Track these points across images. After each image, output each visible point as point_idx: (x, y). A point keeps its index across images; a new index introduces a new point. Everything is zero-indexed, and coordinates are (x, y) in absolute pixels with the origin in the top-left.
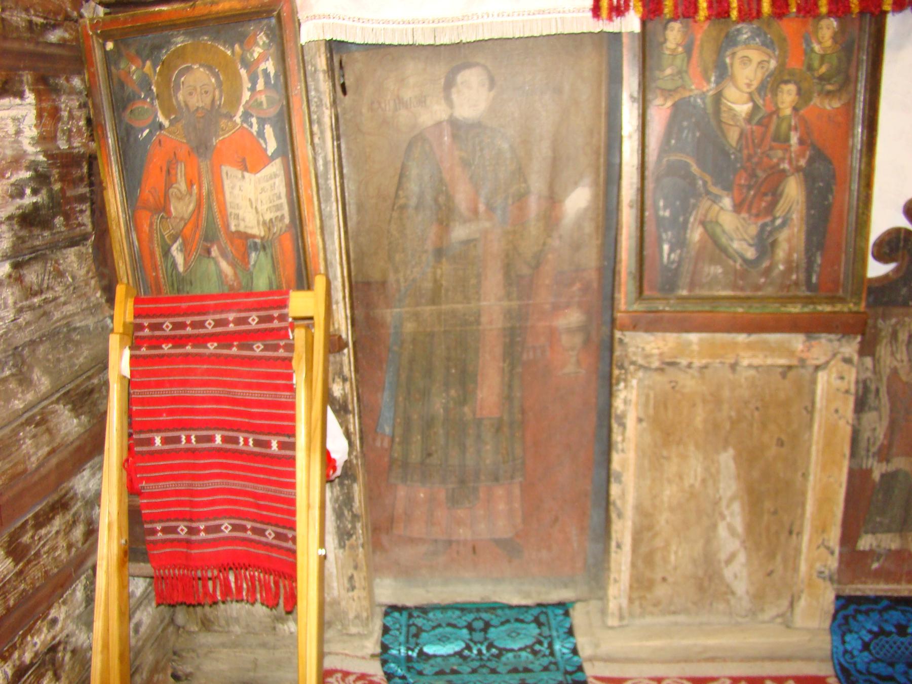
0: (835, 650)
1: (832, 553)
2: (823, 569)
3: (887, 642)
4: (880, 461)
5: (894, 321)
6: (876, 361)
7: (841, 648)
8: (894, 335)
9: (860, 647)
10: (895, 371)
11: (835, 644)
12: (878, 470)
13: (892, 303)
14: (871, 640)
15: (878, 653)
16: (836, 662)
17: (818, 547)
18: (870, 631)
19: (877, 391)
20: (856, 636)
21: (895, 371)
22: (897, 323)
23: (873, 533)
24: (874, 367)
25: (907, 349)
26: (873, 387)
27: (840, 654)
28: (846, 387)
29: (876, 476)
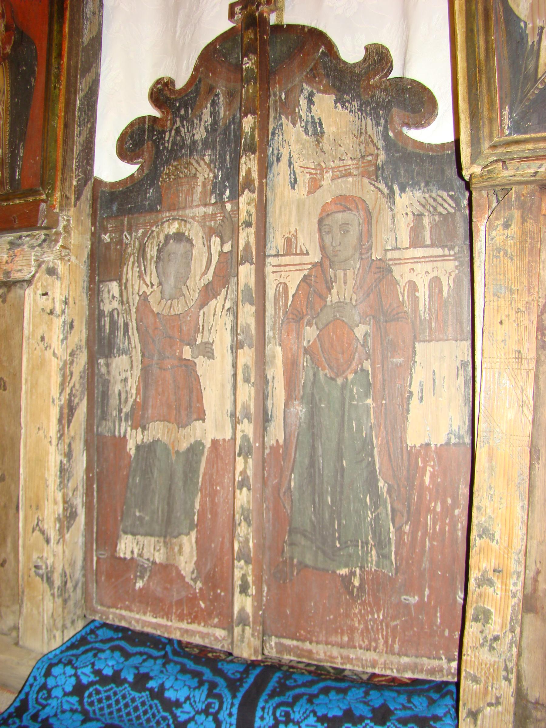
0: (31, 680)
1: (48, 541)
2: (40, 564)
3: (133, 700)
4: (134, 427)
5: (141, 231)
6: (124, 287)
7: (41, 680)
8: (142, 251)
9: (69, 688)
10: (144, 298)
11: (36, 673)
12: (134, 439)
13: (140, 210)
14: (92, 684)
15: (92, 704)
16: (22, 696)
17: (33, 531)
18: (98, 672)
19: (126, 325)
20: (73, 672)
21: (144, 298)
22: (144, 234)
23: (134, 534)
24: (121, 295)
25: (156, 267)
26: (121, 322)
27: (36, 688)
28: (50, 307)
29: (131, 447)
